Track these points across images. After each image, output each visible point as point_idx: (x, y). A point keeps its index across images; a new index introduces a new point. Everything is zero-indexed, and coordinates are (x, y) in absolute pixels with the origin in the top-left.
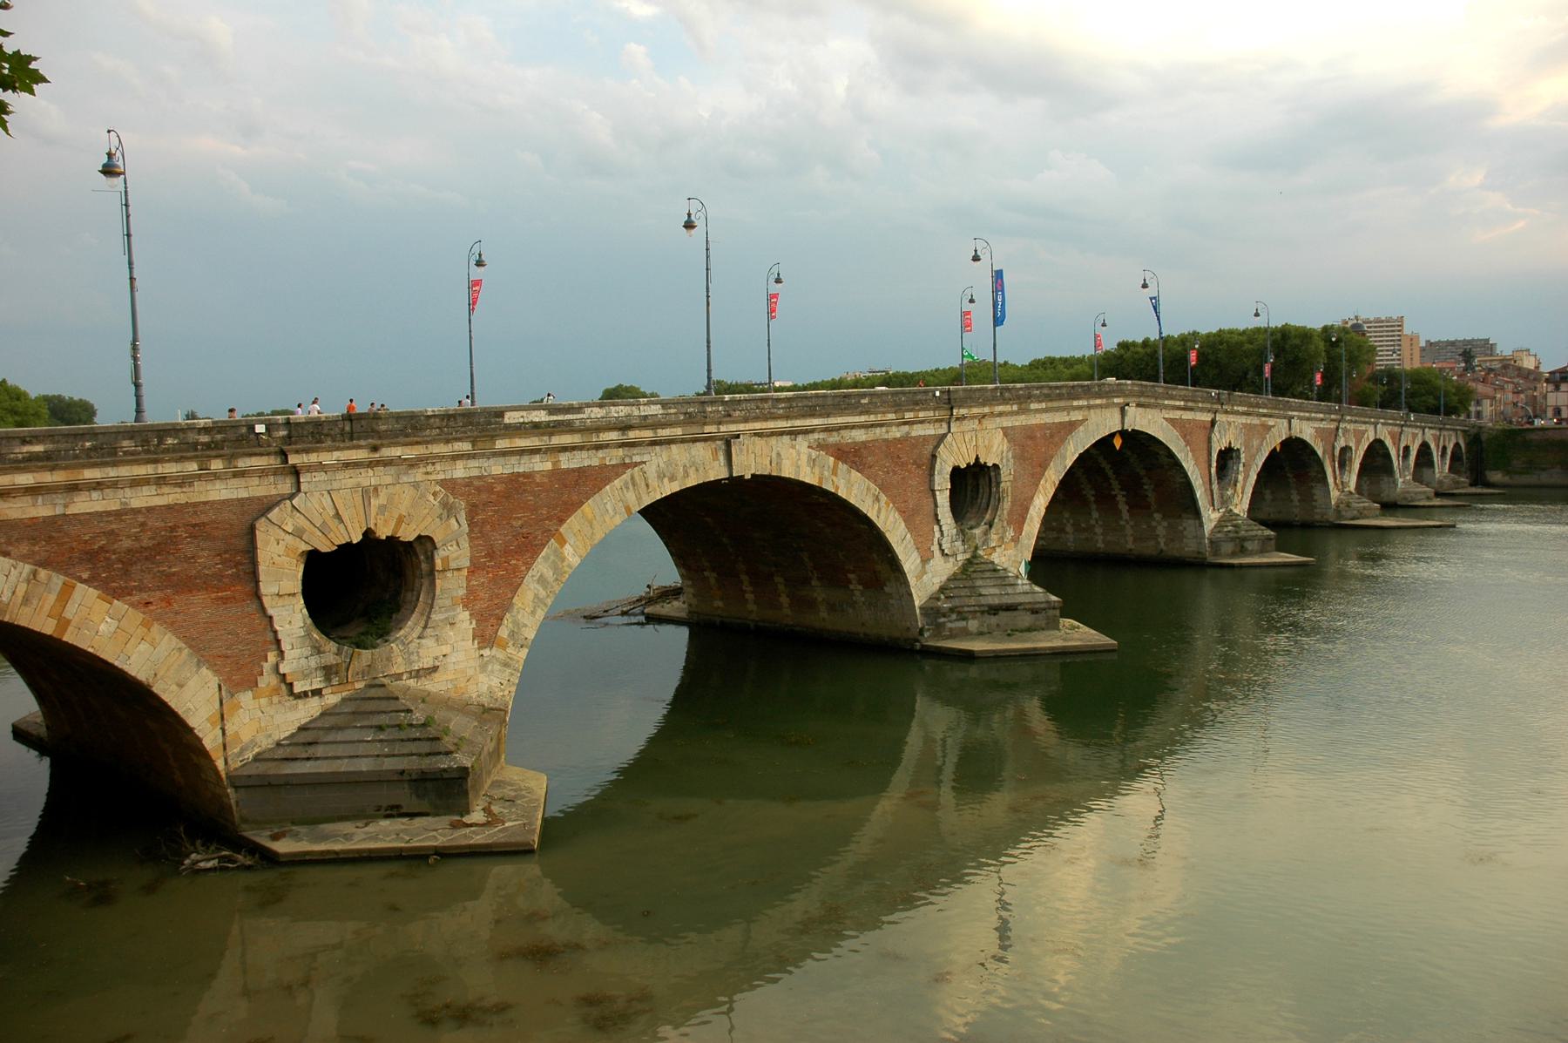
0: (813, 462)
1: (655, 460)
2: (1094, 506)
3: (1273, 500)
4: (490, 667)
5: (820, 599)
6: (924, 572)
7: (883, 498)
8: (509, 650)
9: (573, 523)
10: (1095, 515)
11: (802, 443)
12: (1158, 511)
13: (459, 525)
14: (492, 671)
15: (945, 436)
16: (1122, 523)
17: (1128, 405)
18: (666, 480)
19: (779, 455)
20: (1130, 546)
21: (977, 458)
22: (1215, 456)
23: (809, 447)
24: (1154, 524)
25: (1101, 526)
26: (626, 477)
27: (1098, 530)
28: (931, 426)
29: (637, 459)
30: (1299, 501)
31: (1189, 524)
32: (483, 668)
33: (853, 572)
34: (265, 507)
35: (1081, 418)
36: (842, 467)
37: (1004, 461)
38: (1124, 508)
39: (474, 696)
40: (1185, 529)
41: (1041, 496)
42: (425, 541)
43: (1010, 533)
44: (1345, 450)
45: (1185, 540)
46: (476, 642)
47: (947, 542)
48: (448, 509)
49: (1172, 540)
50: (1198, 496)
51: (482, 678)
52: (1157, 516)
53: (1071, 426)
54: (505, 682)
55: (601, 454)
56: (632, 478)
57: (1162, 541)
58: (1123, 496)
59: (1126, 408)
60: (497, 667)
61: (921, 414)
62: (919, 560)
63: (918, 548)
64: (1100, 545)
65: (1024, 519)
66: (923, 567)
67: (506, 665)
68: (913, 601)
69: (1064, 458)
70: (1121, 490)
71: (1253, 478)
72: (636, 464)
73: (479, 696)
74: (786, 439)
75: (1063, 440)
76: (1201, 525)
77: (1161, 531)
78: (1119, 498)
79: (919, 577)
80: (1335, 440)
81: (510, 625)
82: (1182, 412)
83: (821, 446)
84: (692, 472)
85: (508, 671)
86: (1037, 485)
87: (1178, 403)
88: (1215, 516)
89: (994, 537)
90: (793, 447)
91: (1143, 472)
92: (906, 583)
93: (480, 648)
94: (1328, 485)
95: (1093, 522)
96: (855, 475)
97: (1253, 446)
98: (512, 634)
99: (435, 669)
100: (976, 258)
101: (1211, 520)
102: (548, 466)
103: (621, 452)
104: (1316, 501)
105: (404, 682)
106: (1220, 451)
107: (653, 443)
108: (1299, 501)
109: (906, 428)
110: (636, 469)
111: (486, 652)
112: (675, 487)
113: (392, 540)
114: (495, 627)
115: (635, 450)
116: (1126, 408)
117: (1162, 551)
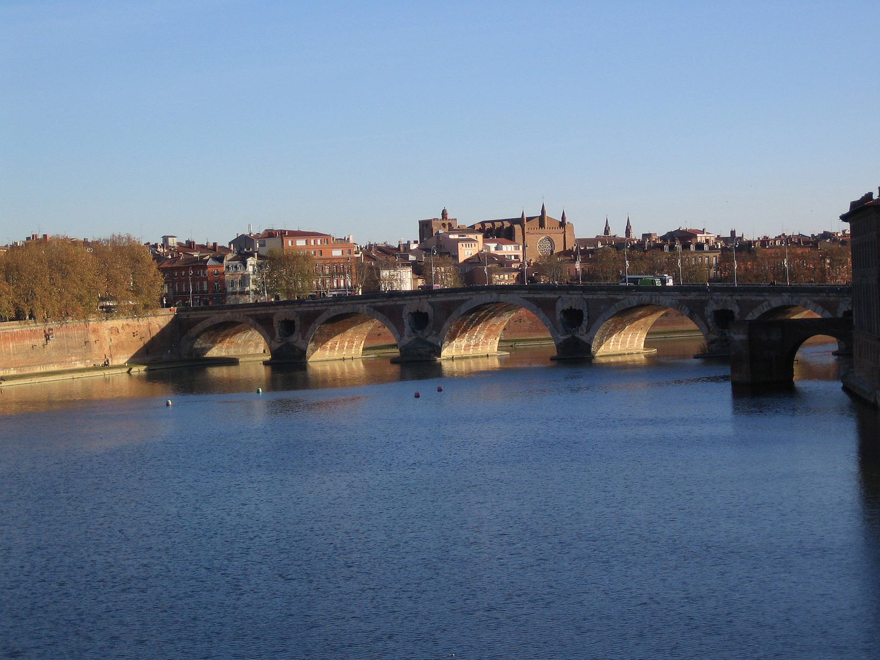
1: (332, 309)
6: (401, 340)
11: (365, 306)
13: (298, 318)
21: (418, 310)
26: (326, 312)
34: (274, 313)
35: (468, 298)
36: (375, 311)
42: (293, 321)
48: (296, 316)
53: (463, 301)
74: (361, 305)
82: (535, 295)
83: (370, 306)
84: (339, 311)
90: (363, 307)
96: (379, 313)
101: (560, 339)
102: (313, 309)
109: (395, 302)
112: (336, 314)
113: (289, 320)
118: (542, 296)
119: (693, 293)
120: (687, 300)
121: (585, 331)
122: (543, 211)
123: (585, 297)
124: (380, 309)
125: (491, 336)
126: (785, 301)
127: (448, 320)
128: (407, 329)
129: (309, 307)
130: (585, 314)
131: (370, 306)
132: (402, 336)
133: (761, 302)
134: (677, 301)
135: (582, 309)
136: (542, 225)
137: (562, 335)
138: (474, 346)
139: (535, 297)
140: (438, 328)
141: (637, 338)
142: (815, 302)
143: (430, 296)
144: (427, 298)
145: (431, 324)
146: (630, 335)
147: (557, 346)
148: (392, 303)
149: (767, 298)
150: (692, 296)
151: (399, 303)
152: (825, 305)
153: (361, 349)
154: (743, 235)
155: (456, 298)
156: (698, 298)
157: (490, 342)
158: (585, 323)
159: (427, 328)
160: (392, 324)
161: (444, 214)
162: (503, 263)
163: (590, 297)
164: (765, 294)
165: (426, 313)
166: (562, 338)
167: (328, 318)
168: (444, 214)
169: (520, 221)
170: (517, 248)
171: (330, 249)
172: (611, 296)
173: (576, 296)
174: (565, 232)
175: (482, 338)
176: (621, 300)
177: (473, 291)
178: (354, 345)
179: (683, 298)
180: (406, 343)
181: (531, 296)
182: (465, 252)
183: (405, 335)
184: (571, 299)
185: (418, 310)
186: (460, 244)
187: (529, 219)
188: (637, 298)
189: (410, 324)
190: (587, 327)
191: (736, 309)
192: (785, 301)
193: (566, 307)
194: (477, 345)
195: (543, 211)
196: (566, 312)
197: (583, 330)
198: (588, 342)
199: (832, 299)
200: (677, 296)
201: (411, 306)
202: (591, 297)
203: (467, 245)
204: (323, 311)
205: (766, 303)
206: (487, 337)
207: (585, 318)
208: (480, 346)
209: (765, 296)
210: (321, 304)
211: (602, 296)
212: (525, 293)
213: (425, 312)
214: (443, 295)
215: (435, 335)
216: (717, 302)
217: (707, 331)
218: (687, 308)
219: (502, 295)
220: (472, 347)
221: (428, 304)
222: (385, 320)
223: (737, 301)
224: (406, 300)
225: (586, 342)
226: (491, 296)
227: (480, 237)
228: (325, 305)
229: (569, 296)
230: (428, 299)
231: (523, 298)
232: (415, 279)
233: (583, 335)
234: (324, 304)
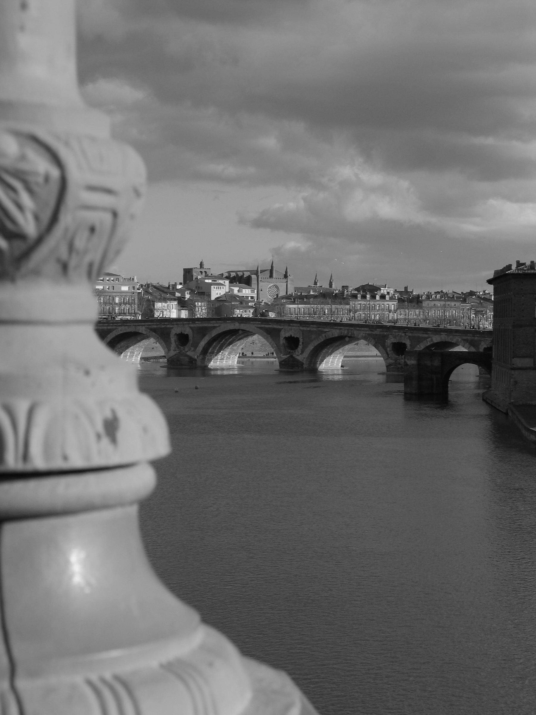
0: (145, 331)
1: (120, 328)
6: (168, 353)
7: (160, 338)
9: (109, 336)
11: (144, 327)
19: (139, 329)
21: (182, 332)
23: (145, 328)
26: (116, 330)
53: (215, 327)
55: (113, 327)
56: (117, 331)
61: (166, 323)
62: (167, 350)
63: (167, 348)
83: (147, 328)
101: (282, 358)
102: (106, 328)
103: (115, 327)
107: (119, 326)
109: (165, 326)
110: (117, 330)
118: (270, 326)
119: (378, 329)
120: (374, 334)
121: (300, 352)
122: (272, 267)
123: (302, 328)
124: (154, 330)
125: (233, 353)
126: (443, 338)
127: (203, 340)
128: (173, 345)
129: (102, 326)
130: (301, 340)
131: (147, 328)
132: (169, 350)
133: (425, 338)
134: (366, 334)
135: (298, 336)
136: (271, 276)
137: (284, 355)
138: (220, 360)
139: (266, 327)
140: (196, 345)
141: (336, 360)
142: (464, 340)
143: (191, 323)
144: (189, 324)
145: (191, 342)
146: (332, 357)
147: (281, 363)
148: (163, 326)
149: (431, 335)
150: (378, 332)
151: (168, 326)
152: (472, 343)
153: (139, 359)
154: (413, 290)
155: (210, 325)
156: (382, 333)
157: (232, 357)
158: (300, 347)
159: (187, 345)
160: (162, 341)
161: (201, 265)
162: (243, 302)
163: (305, 329)
164: (429, 332)
165: (187, 335)
166: (283, 357)
167: (117, 335)
168: (201, 265)
169: (256, 273)
170: (253, 291)
171: (120, 286)
172: (320, 329)
173: (294, 328)
174: (287, 282)
175: (226, 354)
176: (327, 332)
177: (222, 321)
178: (135, 355)
179: (370, 333)
180: (172, 355)
181: (263, 326)
182: (216, 293)
183: (172, 350)
184: (291, 329)
185: (182, 332)
186: (212, 287)
187: (262, 271)
188: (338, 331)
189: (175, 342)
190: (302, 350)
191: (408, 343)
192: (443, 338)
193: (287, 335)
194: (222, 359)
195: (272, 267)
196: (286, 339)
197: (298, 352)
198: (302, 361)
199: (476, 338)
200: (366, 331)
201: (176, 330)
202: (306, 329)
203: (218, 288)
204: (113, 330)
205: (429, 339)
206: (230, 354)
207: (301, 343)
208: (225, 360)
209: (429, 334)
210: (112, 324)
211: (313, 328)
212: (259, 324)
213: (187, 334)
214: (200, 322)
215: (193, 350)
216: (395, 337)
217: (387, 357)
218: (373, 340)
219: (242, 324)
220: (219, 360)
221: (189, 328)
222: (158, 338)
223: (409, 337)
224: (173, 324)
225: (300, 360)
226: (235, 325)
227: (227, 282)
228: (116, 326)
229: (290, 327)
230: (190, 325)
231: (257, 327)
232: (179, 310)
233: (298, 355)
234: (114, 324)
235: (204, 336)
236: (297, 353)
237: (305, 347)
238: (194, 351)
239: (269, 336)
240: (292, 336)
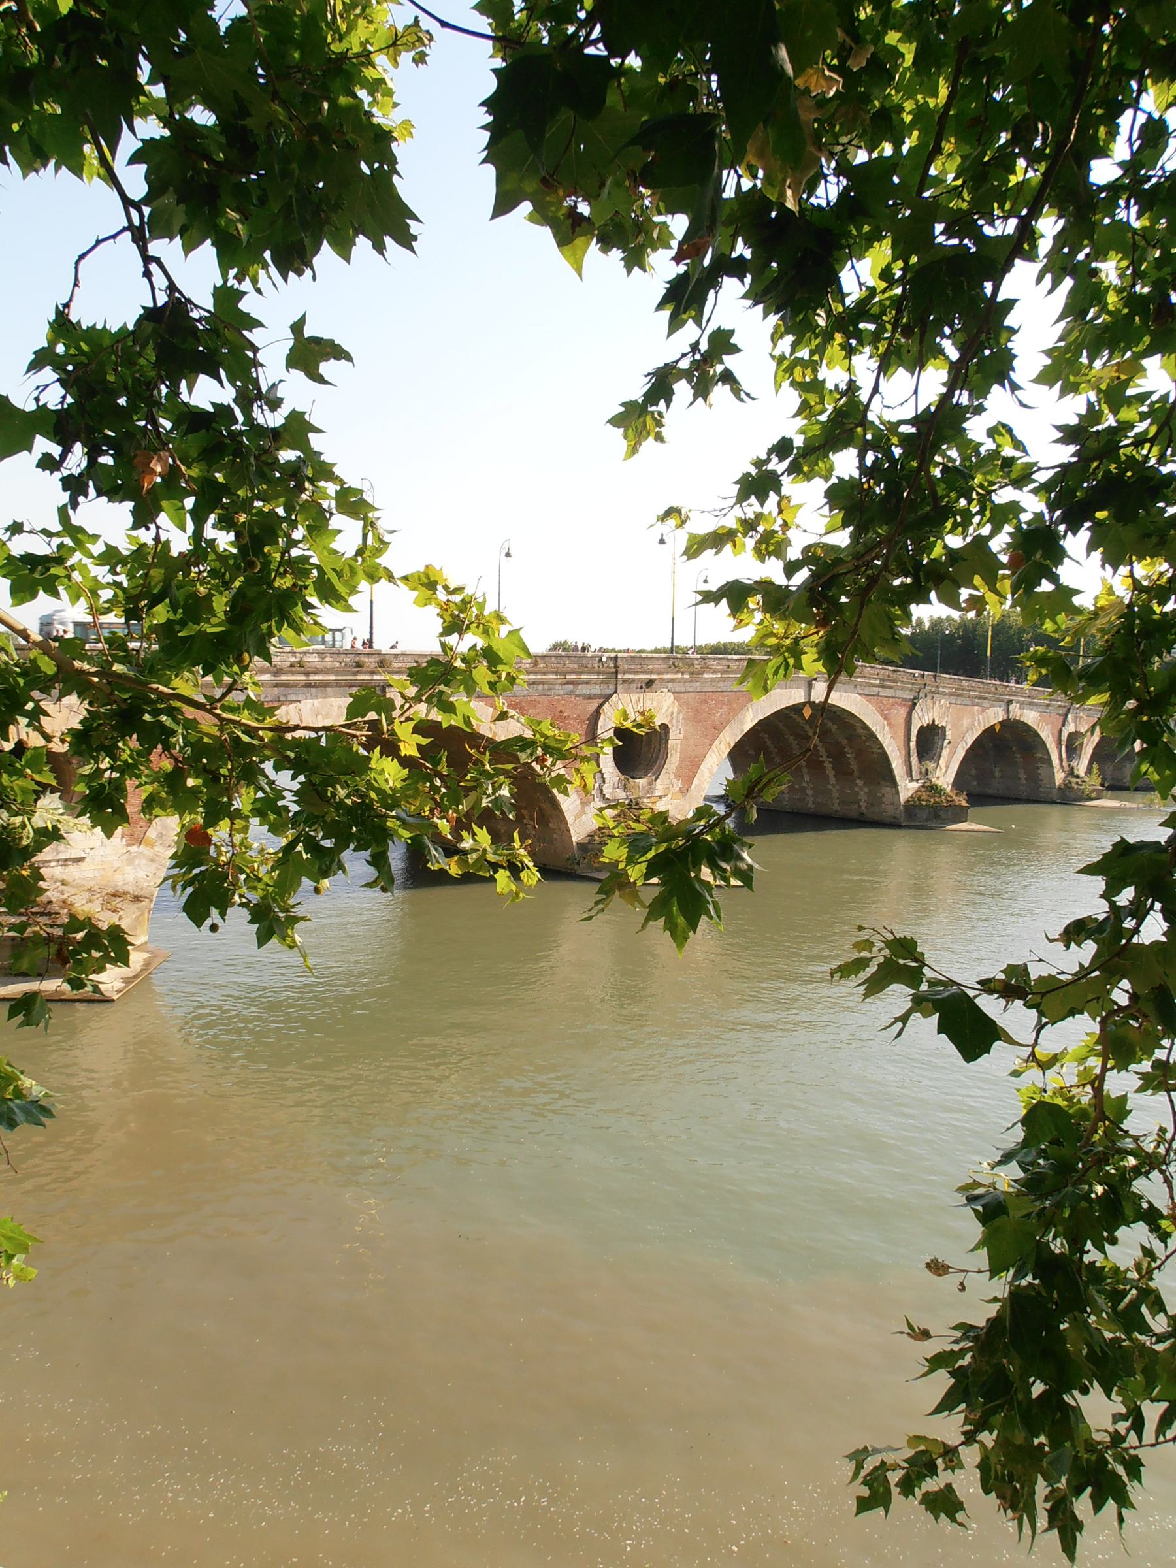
2: (805, 770)
3: (1002, 777)
4: (137, 862)
5: (502, 831)
8: (156, 849)
10: (807, 778)
12: (859, 778)
14: (139, 865)
15: (611, 696)
16: (830, 787)
17: (815, 679)
18: (319, 717)
20: (836, 807)
22: (914, 732)
24: (857, 789)
25: (812, 789)
27: (810, 792)
28: (597, 687)
29: (292, 697)
30: (1026, 779)
31: (887, 790)
32: (130, 862)
33: (525, 808)
37: (674, 721)
38: (831, 773)
39: (120, 884)
40: (883, 795)
41: (714, 756)
43: (678, 785)
44: (1073, 736)
45: (883, 806)
46: (124, 840)
47: (607, 788)
49: (872, 805)
50: (894, 765)
51: (128, 869)
52: (860, 782)
54: (151, 875)
57: (863, 805)
58: (830, 762)
59: (814, 682)
60: (144, 862)
62: (578, 802)
64: (811, 805)
65: (695, 774)
66: (583, 808)
67: (152, 860)
68: (571, 837)
69: (742, 723)
70: (828, 757)
71: (961, 754)
72: (291, 702)
73: (124, 884)
75: (742, 707)
76: (897, 793)
77: (862, 796)
78: (826, 764)
79: (578, 816)
80: (1063, 725)
81: (159, 828)
82: (880, 689)
85: (154, 866)
86: (711, 745)
87: (872, 681)
88: (914, 786)
89: (659, 788)
91: (844, 742)
92: (565, 821)
93: (128, 845)
94: (1052, 767)
95: (804, 784)
97: (962, 725)
98: (161, 835)
99: (81, 859)
100: (662, 541)
101: (908, 790)
104: (1041, 780)
105: (49, 869)
106: (922, 727)
107: (308, 685)
108: (1026, 779)
111: (134, 849)
114: (145, 829)
115: (290, 691)
116: (814, 682)
117: (862, 814)
121: (944, 769)
135: (944, 724)
140: (688, 773)
145: (674, 760)
158: (945, 752)
193: (926, 721)
215: (681, 791)
235: (718, 729)
236: (938, 773)
237: (953, 753)
238: (684, 792)
239: (885, 722)
240: (936, 723)
